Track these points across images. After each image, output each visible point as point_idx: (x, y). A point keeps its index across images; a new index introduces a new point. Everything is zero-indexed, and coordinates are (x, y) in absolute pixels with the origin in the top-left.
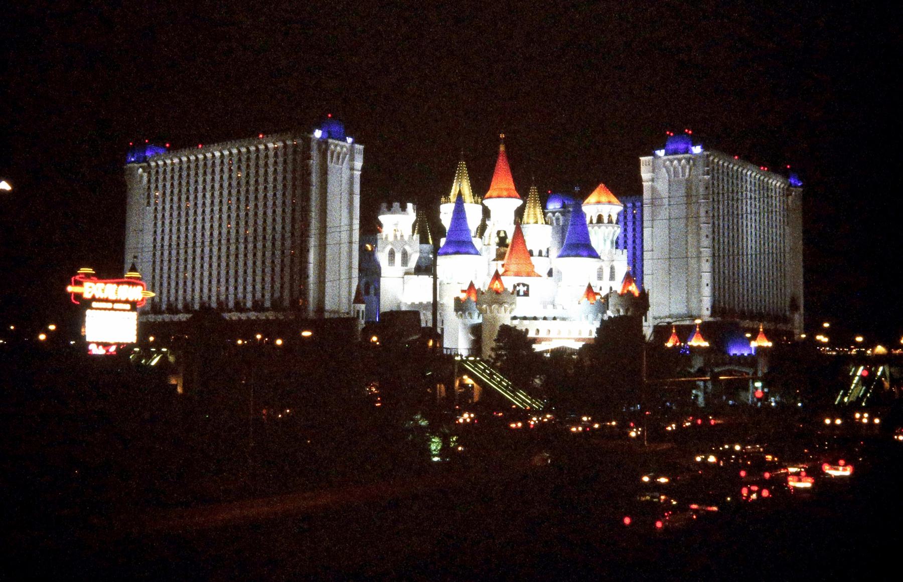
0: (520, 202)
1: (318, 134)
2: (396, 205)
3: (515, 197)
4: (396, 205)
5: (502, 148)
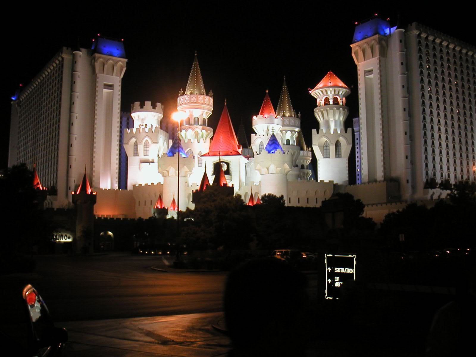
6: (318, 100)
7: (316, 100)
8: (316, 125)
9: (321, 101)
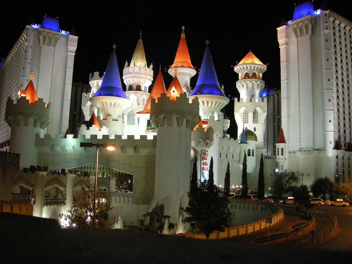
0: (193, 72)
1: (35, 26)
2: (97, 74)
4: (97, 74)
5: (183, 35)
6: (240, 75)
7: (238, 75)
8: (237, 95)
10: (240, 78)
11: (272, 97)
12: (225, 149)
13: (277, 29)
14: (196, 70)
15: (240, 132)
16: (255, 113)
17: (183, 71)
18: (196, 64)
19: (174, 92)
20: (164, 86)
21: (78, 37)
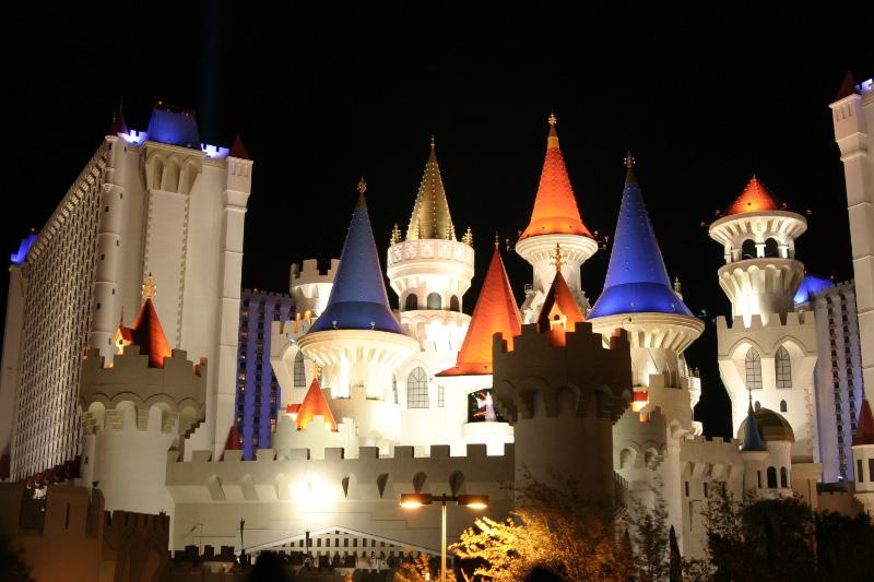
0: (587, 247)
1: (132, 137)
2: (311, 264)
3: (579, 233)
4: (311, 264)
5: (553, 142)
6: (727, 250)
8: (723, 306)
9: (731, 250)
10: (728, 258)
11: (825, 302)
12: (700, 468)
13: (831, 106)
14: (596, 239)
15: (739, 416)
16: (781, 359)
17: (556, 246)
18: (597, 219)
19: (557, 318)
20: (511, 291)
21: (252, 162)
